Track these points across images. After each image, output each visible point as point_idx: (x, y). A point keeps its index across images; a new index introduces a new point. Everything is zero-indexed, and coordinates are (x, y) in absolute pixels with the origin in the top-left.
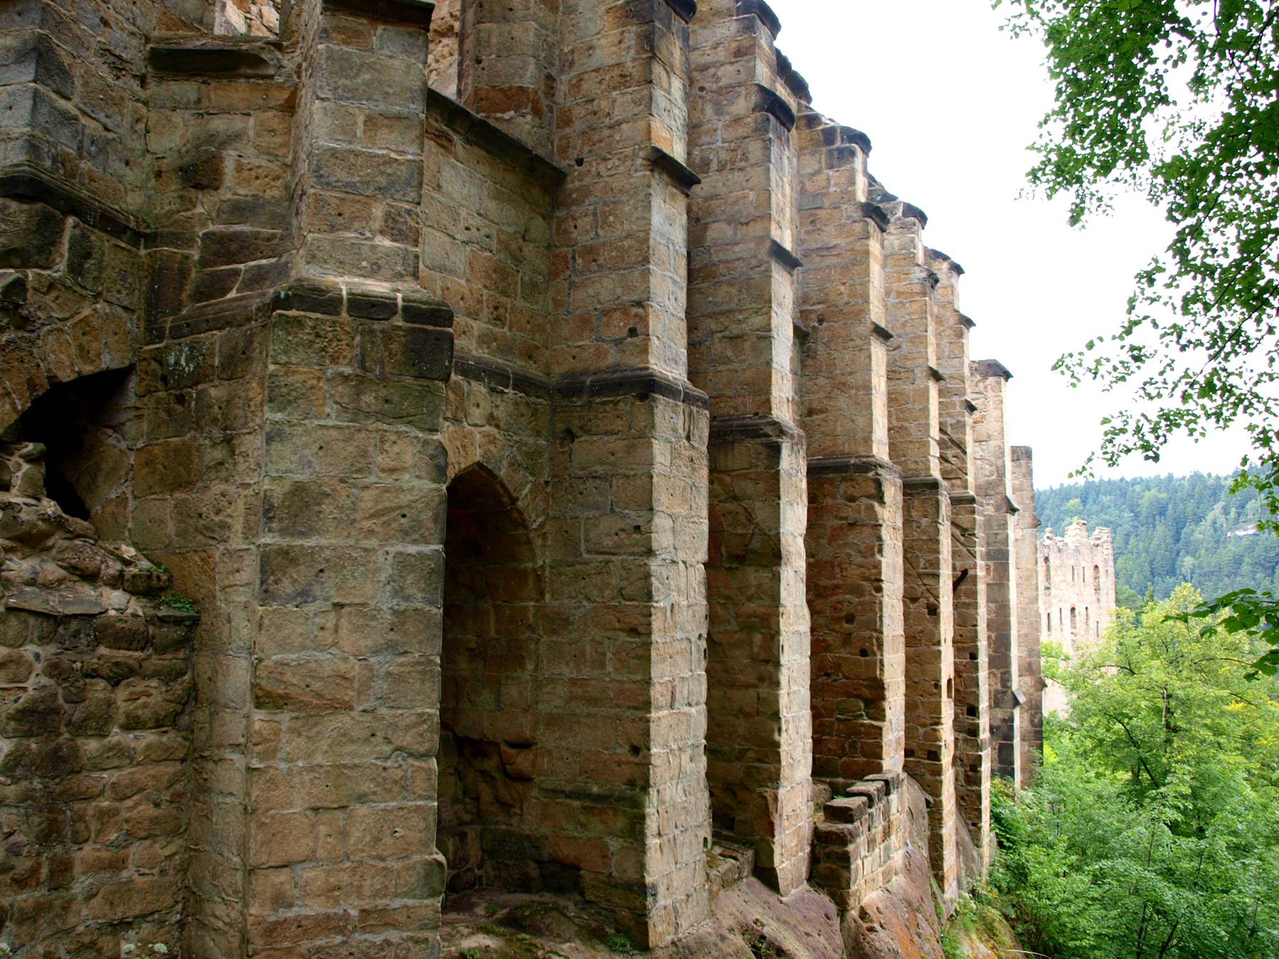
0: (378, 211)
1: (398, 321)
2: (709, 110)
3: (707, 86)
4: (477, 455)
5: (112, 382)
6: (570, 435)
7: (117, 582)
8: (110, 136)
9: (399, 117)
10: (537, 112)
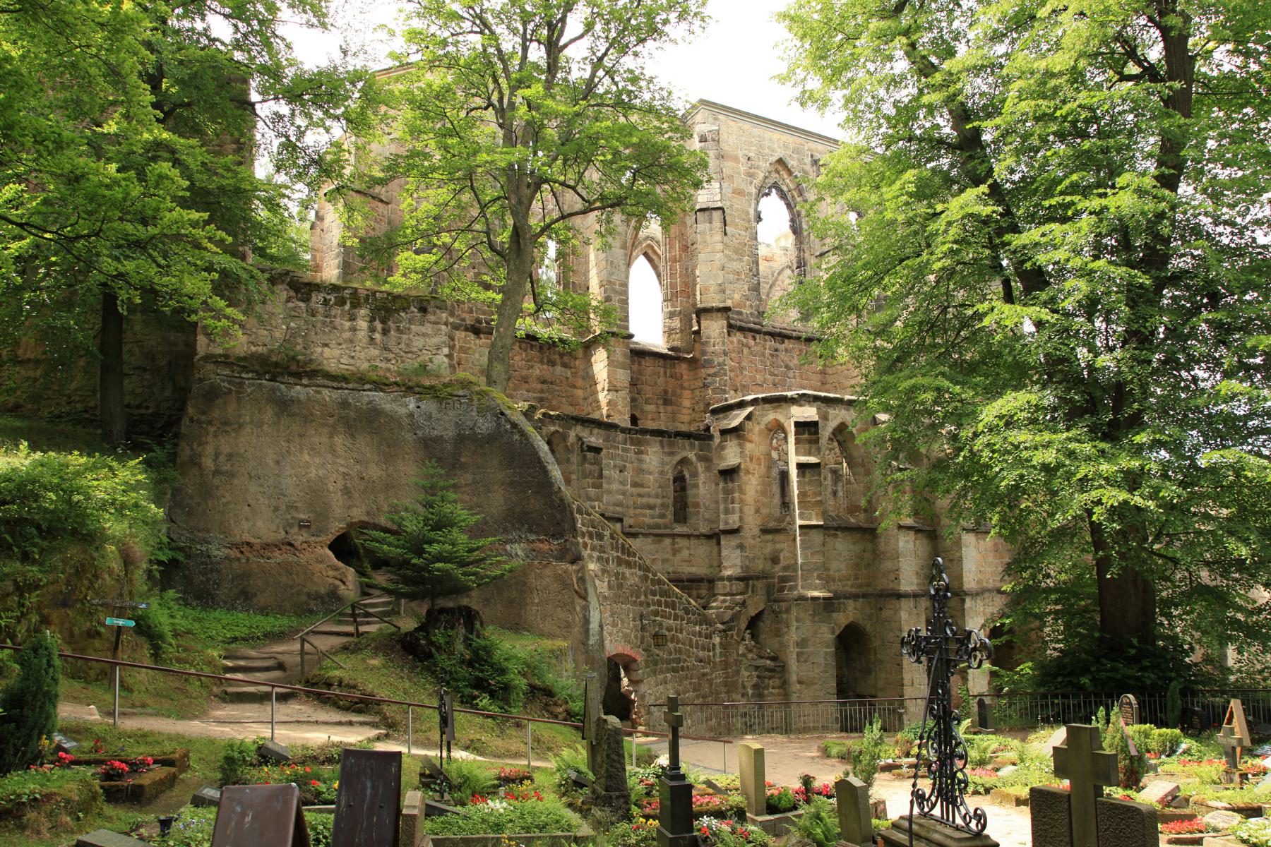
4: (851, 619)
5: (761, 612)
6: (881, 609)
7: (768, 658)
10: (865, 511)
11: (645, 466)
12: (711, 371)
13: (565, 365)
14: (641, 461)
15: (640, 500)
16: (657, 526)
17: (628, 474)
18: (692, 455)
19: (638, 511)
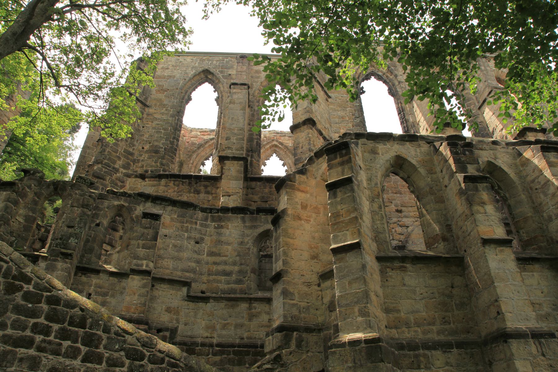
0: (356, 309)
1: (363, 345)
2: (542, 196)
3: (537, 187)
8: (309, 304)
9: (357, 278)
10: (444, 239)
11: (223, 239)
13: (208, 193)
14: (219, 234)
15: (215, 268)
16: (233, 291)
17: (206, 246)
19: (211, 278)
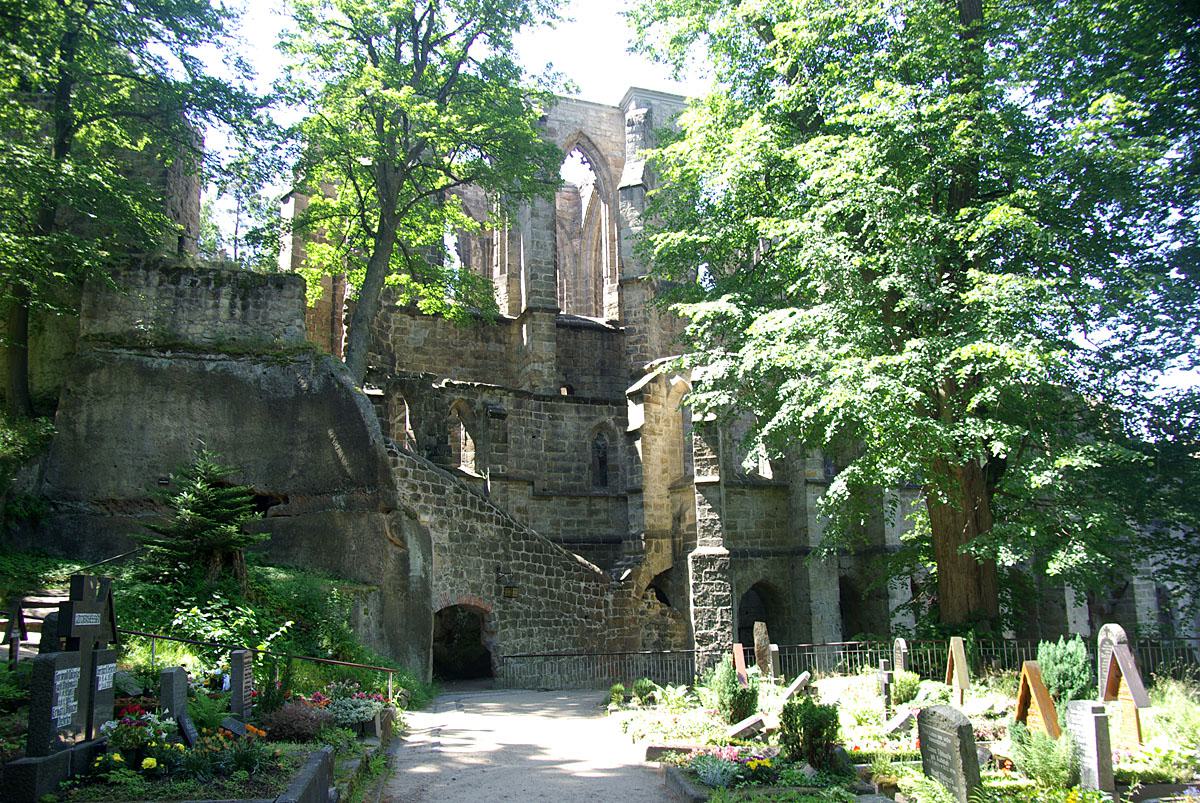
12: (633, 338)
13: (499, 341)
16: (573, 488)
18: (610, 420)
